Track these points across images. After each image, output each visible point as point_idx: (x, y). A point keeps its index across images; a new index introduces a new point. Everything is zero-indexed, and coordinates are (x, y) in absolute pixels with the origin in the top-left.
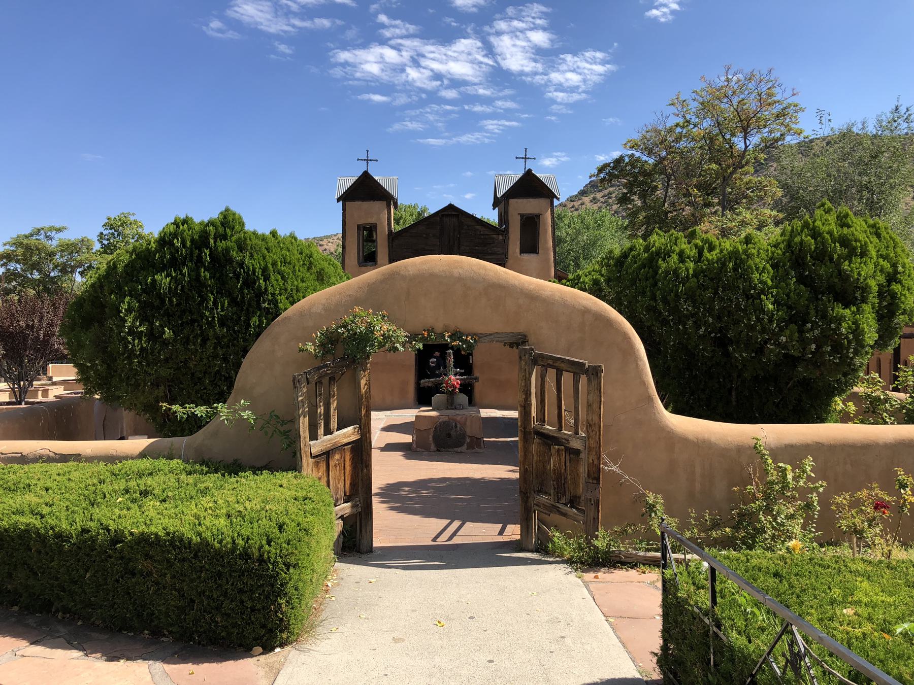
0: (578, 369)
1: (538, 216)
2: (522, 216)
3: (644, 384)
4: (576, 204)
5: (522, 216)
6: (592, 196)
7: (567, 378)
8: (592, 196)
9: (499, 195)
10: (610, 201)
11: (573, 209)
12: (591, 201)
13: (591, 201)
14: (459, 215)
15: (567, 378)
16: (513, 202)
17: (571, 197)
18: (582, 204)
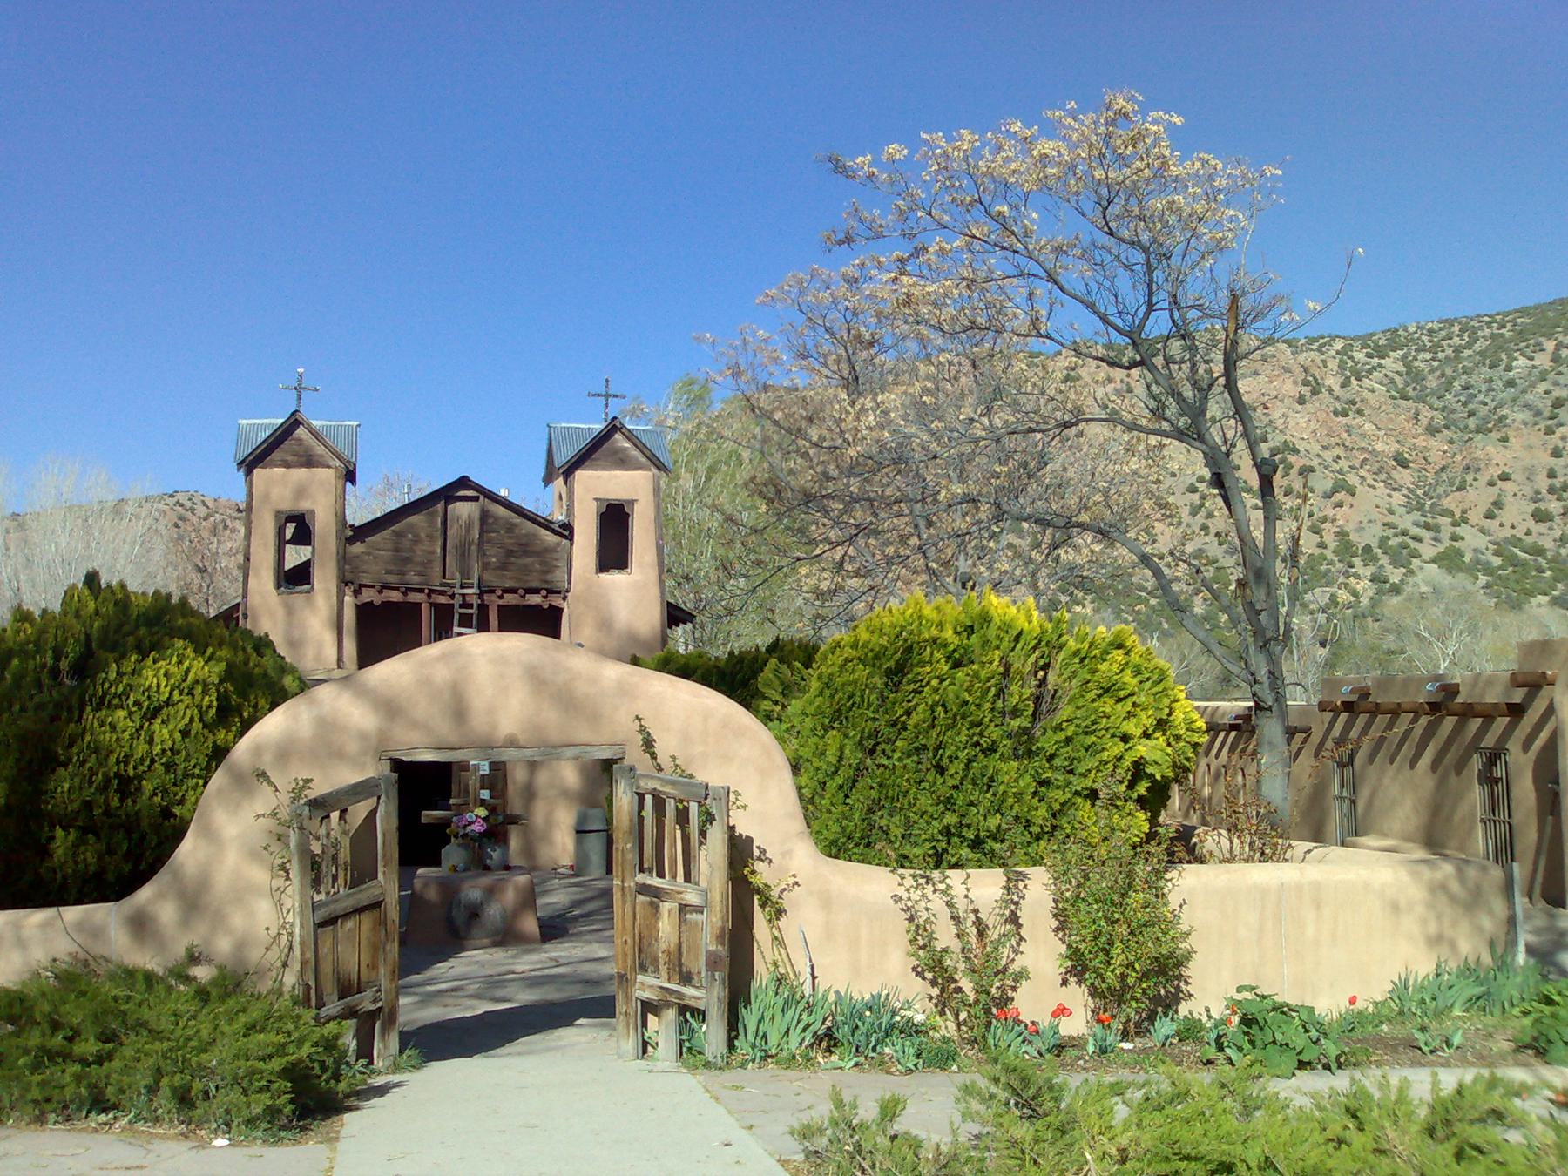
1: (632, 502)
9: (557, 464)
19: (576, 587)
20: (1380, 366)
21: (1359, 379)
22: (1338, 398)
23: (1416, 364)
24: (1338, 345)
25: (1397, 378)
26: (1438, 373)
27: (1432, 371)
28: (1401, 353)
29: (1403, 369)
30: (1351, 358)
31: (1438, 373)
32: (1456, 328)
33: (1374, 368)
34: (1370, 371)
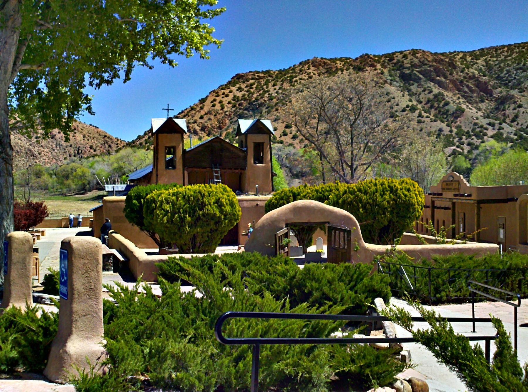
0: (344, 231)
2: (255, 143)
3: (359, 235)
4: (227, 91)
5: (255, 143)
6: (238, 86)
7: (342, 233)
8: (238, 86)
10: (252, 90)
11: (224, 96)
12: (237, 90)
13: (237, 90)
14: (221, 142)
15: (342, 233)
16: (250, 136)
17: (221, 86)
18: (231, 92)
19: (248, 168)
20: (477, 63)
21: (468, 68)
22: (460, 76)
23: (490, 62)
24: (461, 55)
25: (483, 68)
26: (497, 66)
27: (496, 65)
28: (485, 58)
29: (485, 64)
30: (466, 60)
31: (497, 66)
32: (506, 49)
33: (474, 64)
34: (472, 65)
